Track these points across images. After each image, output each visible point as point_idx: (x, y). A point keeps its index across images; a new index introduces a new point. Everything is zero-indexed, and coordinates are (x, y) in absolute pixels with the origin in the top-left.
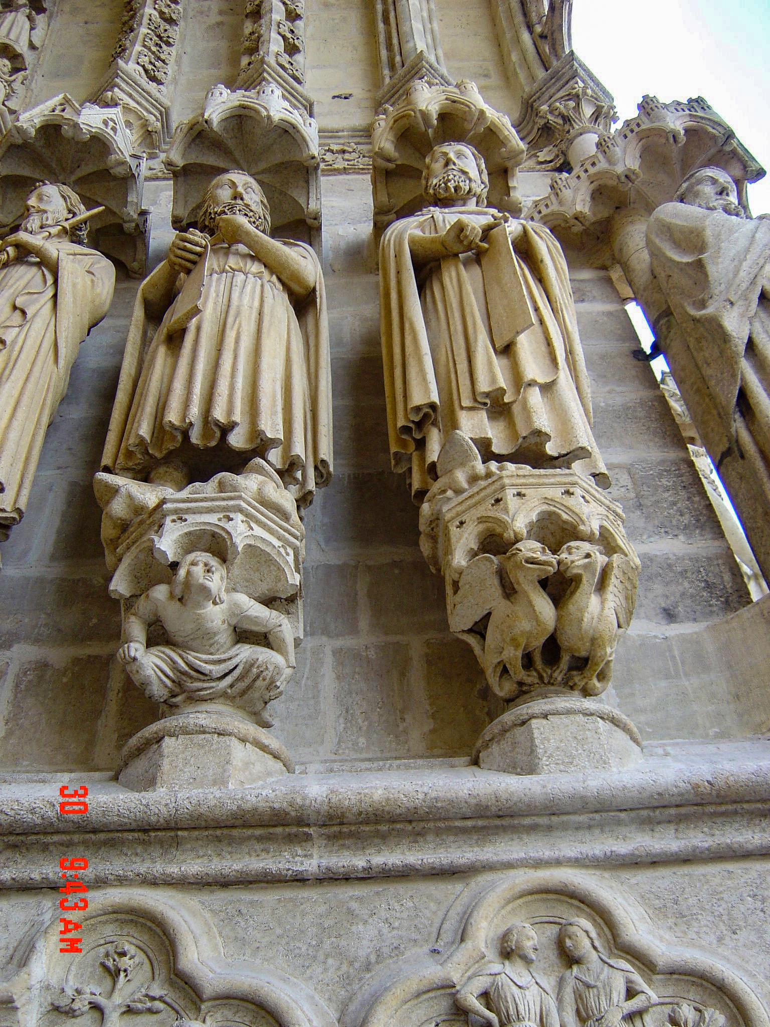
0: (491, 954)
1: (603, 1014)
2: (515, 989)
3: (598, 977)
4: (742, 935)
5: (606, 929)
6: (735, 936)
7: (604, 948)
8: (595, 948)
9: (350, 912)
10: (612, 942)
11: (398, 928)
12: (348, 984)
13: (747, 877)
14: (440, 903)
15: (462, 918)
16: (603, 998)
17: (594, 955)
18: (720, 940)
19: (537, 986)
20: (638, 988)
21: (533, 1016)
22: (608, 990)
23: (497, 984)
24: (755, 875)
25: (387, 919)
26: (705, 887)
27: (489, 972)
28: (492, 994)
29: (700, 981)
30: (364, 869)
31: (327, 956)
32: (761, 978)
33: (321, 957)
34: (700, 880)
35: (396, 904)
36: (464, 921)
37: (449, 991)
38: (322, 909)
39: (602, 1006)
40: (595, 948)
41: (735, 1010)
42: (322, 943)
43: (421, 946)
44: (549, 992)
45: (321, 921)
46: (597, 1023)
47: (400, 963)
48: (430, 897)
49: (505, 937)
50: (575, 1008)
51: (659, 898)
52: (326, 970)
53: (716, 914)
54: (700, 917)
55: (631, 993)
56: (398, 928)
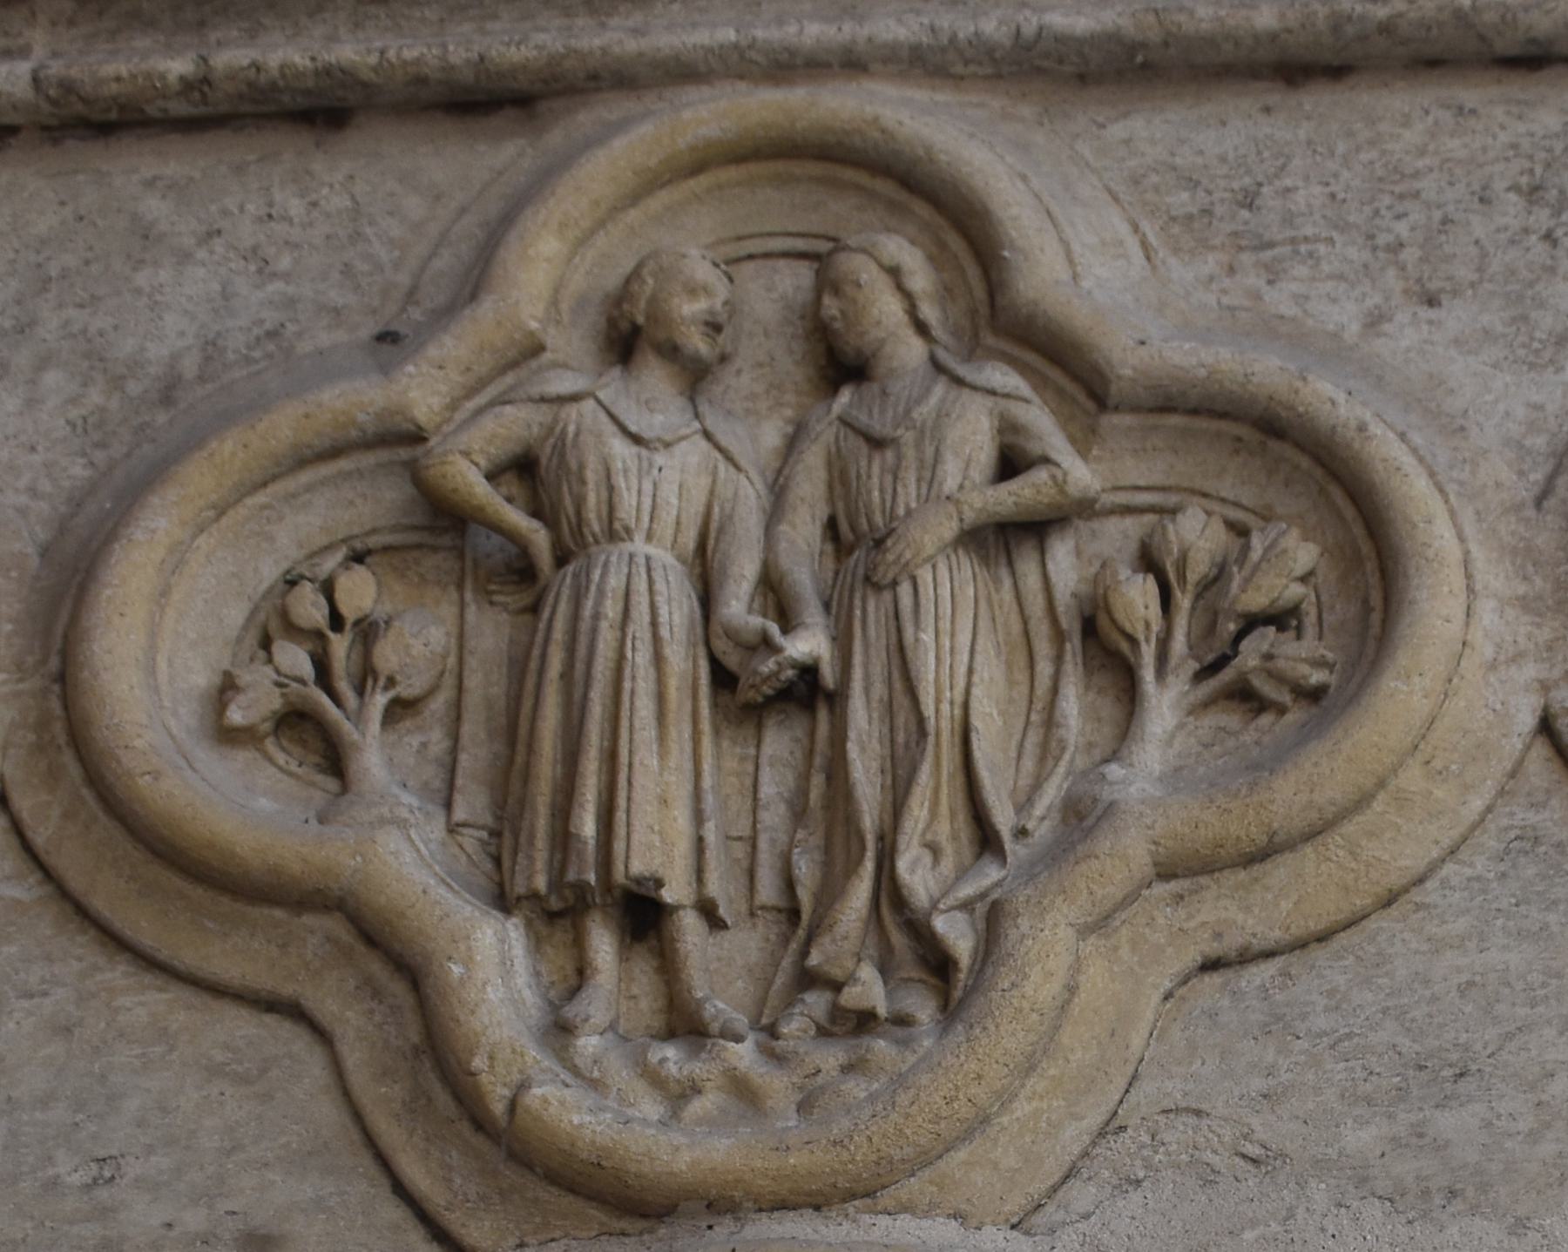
2: (620, 449)
3: (908, 412)
5: (973, 272)
6: (1432, 314)
7: (956, 333)
9: (146, 234)
11: (286, 277)
12: (97, 445)
13: (1522, 128)
14: (438, 198)
16: (910, 477)
17: (912, 351)
19: (704, 444)
20: (1034, 448)
22: (929, 451)
26: (1364, 156)
28: (544, 461)
30: (188, 86)
31: (44, 363)
37: (404, 453)
40: (922, 328)
41: (1358, 530)
44: (743, 463)
50: (822, 512)
51: (1193, 184)
52: (32, 403)
53: (1382, 239)
55: (1010, 464)
56: (286, 277)
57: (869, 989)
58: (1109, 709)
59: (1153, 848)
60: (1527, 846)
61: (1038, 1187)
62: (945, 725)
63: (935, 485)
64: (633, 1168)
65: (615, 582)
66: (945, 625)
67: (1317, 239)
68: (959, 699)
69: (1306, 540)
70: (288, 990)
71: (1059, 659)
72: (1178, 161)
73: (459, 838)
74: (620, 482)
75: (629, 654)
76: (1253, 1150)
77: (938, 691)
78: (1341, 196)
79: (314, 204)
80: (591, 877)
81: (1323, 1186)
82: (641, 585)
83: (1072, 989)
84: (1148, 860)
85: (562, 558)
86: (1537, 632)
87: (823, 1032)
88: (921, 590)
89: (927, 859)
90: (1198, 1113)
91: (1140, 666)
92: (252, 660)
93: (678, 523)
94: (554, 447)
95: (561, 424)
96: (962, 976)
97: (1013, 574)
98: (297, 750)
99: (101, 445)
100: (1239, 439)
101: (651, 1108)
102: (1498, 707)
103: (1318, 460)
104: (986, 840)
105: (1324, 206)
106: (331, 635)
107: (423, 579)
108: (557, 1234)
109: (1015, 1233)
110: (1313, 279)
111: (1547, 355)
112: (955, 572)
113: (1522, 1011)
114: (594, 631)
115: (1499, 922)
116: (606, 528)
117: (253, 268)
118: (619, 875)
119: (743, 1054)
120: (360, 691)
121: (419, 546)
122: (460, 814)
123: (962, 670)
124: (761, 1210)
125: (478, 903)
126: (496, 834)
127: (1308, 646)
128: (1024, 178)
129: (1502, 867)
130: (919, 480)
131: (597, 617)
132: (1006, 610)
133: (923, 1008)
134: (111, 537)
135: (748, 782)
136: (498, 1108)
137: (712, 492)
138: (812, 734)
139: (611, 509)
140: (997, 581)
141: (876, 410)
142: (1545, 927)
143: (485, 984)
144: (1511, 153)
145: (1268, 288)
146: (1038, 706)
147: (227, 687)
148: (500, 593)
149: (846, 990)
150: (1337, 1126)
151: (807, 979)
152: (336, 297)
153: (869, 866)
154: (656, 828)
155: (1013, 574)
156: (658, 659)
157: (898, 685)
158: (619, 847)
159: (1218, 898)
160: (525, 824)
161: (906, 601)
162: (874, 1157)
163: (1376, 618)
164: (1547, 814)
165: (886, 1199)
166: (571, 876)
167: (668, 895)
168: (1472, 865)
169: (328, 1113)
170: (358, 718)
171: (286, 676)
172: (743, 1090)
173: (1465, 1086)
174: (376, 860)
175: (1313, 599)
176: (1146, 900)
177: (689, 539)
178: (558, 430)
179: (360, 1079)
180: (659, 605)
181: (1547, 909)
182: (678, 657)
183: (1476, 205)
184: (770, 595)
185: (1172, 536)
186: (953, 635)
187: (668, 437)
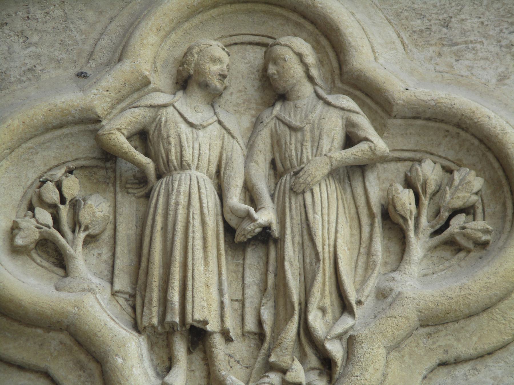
1: (303, 166)
2: (184, 128)
3: (306, 116)
5: (332, 54)
7: (325, 80)
8: (310, 79)
14: (101, 13)
16: (308, 145)
17: (307, 89)
19: (218, 126)
20: (362, 134)
21: (204, 164)
22: (317, 134)
23: (160, 118)
27: (148, 103)
28: (151, 132)
35: (39, 12)
37: (91, 127)
39: (305, 155)
40: (310, 79)
41: (500, 173)
43: (66, 69)
46: (294, 178)
50: (269, 157)
51: (423, 17)
56: (36, 45)
58: (395, 248)
59: (419, 314)
62: (327, 255)
63: (320, 149)
65: (184, 188)
66: (325, 211)
68: (332, 243)
69: (477, 176)
70: (43, 365)
72: (416, 6)
73: (117, 298)
74: (185, 143)
75: (191, 221)
77: (323, 240)
78: (486, 23)
79: (48, 13)
80: (177, 320)
82: (195, 190)
83: (385, 375)
84: (416, 319)
88: (315, 195)
89: (320, 314)
91: (408, 230)
92: (25, 216)
93: (209, 162)
94: (156, 126)
95: (159, 117)
96: (338, 369)
97: (351, 186)
98: (45, 256)
100: (447, 131)
103: (481, 141)
105: (479, 27)
106: (61, 206)
107: (98, 181)
110: (475, 59)
112: (329, 189)
114: (176, 210)
116: (179, 163)
117: (21, 40)
118: (189, 320)
120: (73, 231)
121: (97, 167)
123: (333, 230)
125: (130, 331)
126: (133, 296)
127: (480, 224)
128: (353, 14)
130: (312, 146)
131: (177, 204)
132: (349, 202)
135: (240, 275)
137: (222, 148)
138: (267, 255)
139: (182, 156)
140: (344, 189)
141: (292, 115)
143: (132, 367)
145: (456, 63)
146: (364, 245)
148: (132, 188)
149: (288, 373)
152: (58, 54)
153: (296, 317)
154: (205, 299)
155: (351, 186)
156: (203, 223)
157: (306, 237)
158: (189, 306)
159: (446, 335)
160: (147, 294)
166: (168, 319)
167: (209, 328)
170: (73, 243)
171: (41, 224)
174: (84, 309)
175: (480, 201)
176: (415, 335)
177: (213, 169)
178: (157, 120)
180: (203, 198)
184: (247, 193)
185: (420, 173)
186: (329, 215)
187: (205, 124)
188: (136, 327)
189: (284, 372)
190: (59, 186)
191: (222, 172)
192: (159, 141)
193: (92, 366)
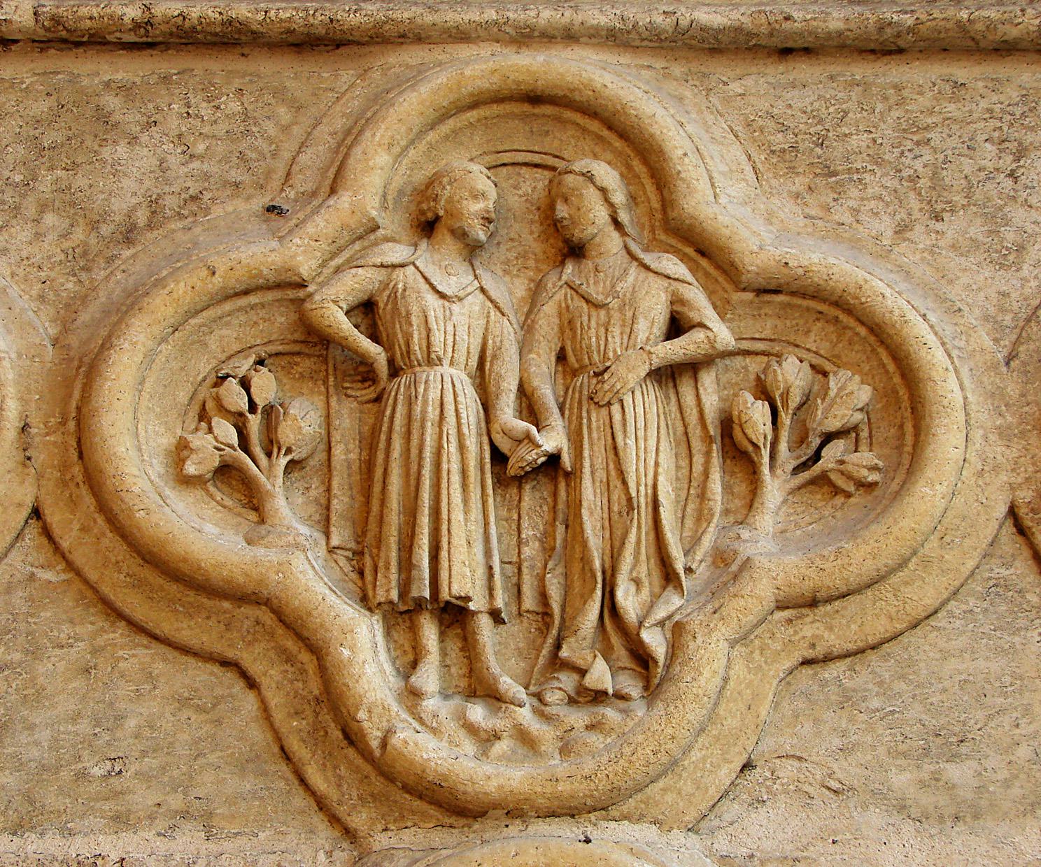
0: (391, 223)
1: (608, 364)
2: (432, 301)
3: (613, 286)
4: (952, 227)
5: (650, 188)
6: (939, 226)
8: (617, 224)
9: (103, 118)
10: (659, 216)
12: (82, 269)
13: (995, 98)
14: (299, 108)
15: (339, 145)
16: (616, 330)
17: (613, 242)
18: (902, 230)
19: (481, 296)
20: (694, 316)
21: (461, 357)
22: (629, 314)
23: (395, 285)
24: (1015, 95)
25: (180, 136)
27: (378, 261)
28: (381, 305)
29: (834, 312)
30: (136, 25)
31: (43, 207)
32: (972, 317)
33: (30, 208)
34: (885, 98)
35: (204, 105)
36: (343, 150)
37: (291, 294)
38: (42, 107)
39: (611, 346)
40: (617, 224)
41: (897, 379)
42: (35, 179)
43: (249, 198)
44: (505, 311)
45: (37, 133)
46: (594, 381)
47: (197, 230)
48: (280, 93)
49: (427, 191)
51: (783, 129)
52: (38, 236)
54: (868, 178)
55: (676, 327)
56: (201, 157)
57: (600, 675)
58: (742, 488)
59: (776, 591)
60: (1001, 590)
61: (704, 807)
62: (642, 500)
63: (633, 337)
64: (462, 788)
65: (434, 394)
66: (641, 433)
67: (865, 170)
68: (650, 482)
69: (862, 383)
70: (231, 654)
71: (708, 454)
72: (776, 111)
73: (334, 556)
74: (433, 326)
75: (445, 446)
76: (835, 785)
77: (638, 477)
78: (879, 141)
79: (218, 108)
80: (427, 594)
81: (877, 810)
83: (726, 680)
84: (773, 599)
85: (395, 372)
86: (1008, 452)
87: (572, 701)
88: (626, 410)
89: (633, 588)
90: (800, 759)
91: (761, 464)
92: (197, 429)
93: (468, 352)
94: (389, 296)
95: (393, 283)
96: (659, 670)
97: (677, 393)
98: (226, 489)
99: (86, 269)
100: (821, 313)
101: (469, 747)
102: (984, 501)
103: (871, 330)
104: (669, 576)
105: (868, 147)
106: (249, 416)
107: (302, 376)
108: (409, 824)
109: (690, 833)
110: (862, 199)
111: (1011, 258)
112: (646, 399)
113: (1000, 700)
114: (423, 427)
115: (984, 641)
116: (425, 356)
117: (179, 151)
118: (445, 595)
119: (525, 715)
121: (298, 354)
122: (335, 541)
123: (652, 463)
124: (538, 817)
125: (358, 607)
126: (359, 554)
127: (866, 457)
128: (682, 125)
129: (985, 605)
130: (622, 334)
132: (673, 416)
133: (633, 687)
134: (107, 345)
135: (514, 527)
136: (375, 744)
137: (487, 329)
138: (555, 495)
139: (429, 347)
140: (667, 397)
141: (591, 282)
142: (1013, 646)
143: (364, 662)
144: (987, 116)
145: (834, 203)
146: (694, 484)
147: (181, 450)
148: (352, 388)
149: (588, 676)
150: (886, 771)
151: (557, 663)
152: (234, 175)
153: (599, 592)
154: (467, 563)
155: (677, 393)
156: (462, 447)
158: (444, 575)
159: (812, 622)
160: (382, 554)
161: (617, 417)
162: (609, 787)
163: (909, 439)
164: (1012, 571)
165: (614, 812)
166: (415, 593)
167: (472, 606)
168: (967, 603)
169: (258, 734)
170: (270, 474)
171: (222, 443)
172: (524, 737)
173: (964, 749)
174: (291, 576)
175: (866, 420)
176: (770, 622)
177: (474, 362)
178: (391, 285)
179: (278, 716)
180: (461, 411)
181: (1014, 634)
182: (471, 443)
183: (966, 151)
184: (524, 399)
185: (780, 378)
186: (646, 440)
187: (461, 294)
188: (364, 600)
189: (583, 672)
190: (245, 384)
191: (487, 367)
192: (394, 324)
193: (305, 657)
